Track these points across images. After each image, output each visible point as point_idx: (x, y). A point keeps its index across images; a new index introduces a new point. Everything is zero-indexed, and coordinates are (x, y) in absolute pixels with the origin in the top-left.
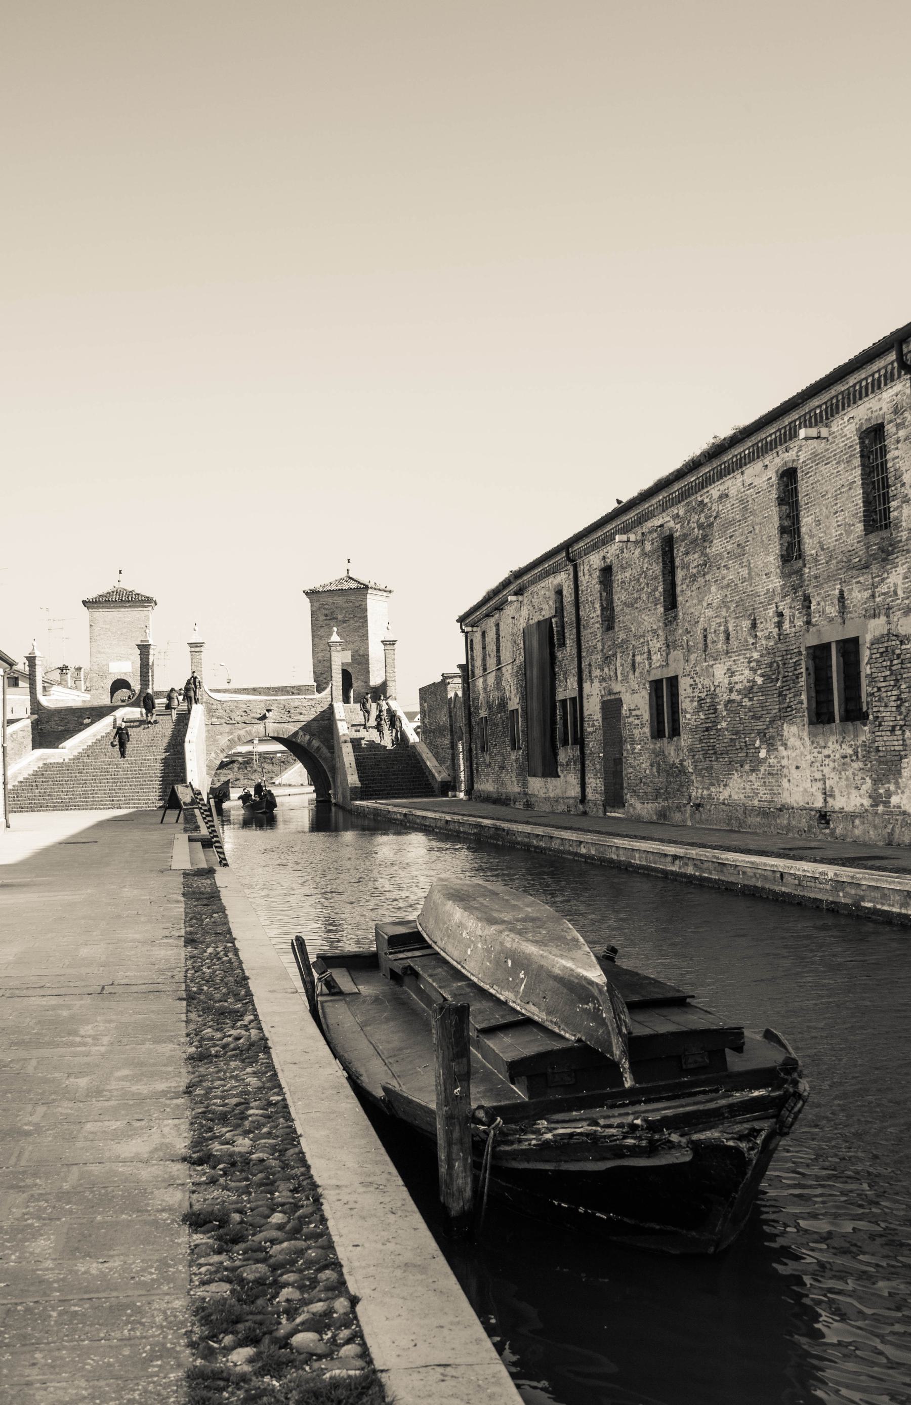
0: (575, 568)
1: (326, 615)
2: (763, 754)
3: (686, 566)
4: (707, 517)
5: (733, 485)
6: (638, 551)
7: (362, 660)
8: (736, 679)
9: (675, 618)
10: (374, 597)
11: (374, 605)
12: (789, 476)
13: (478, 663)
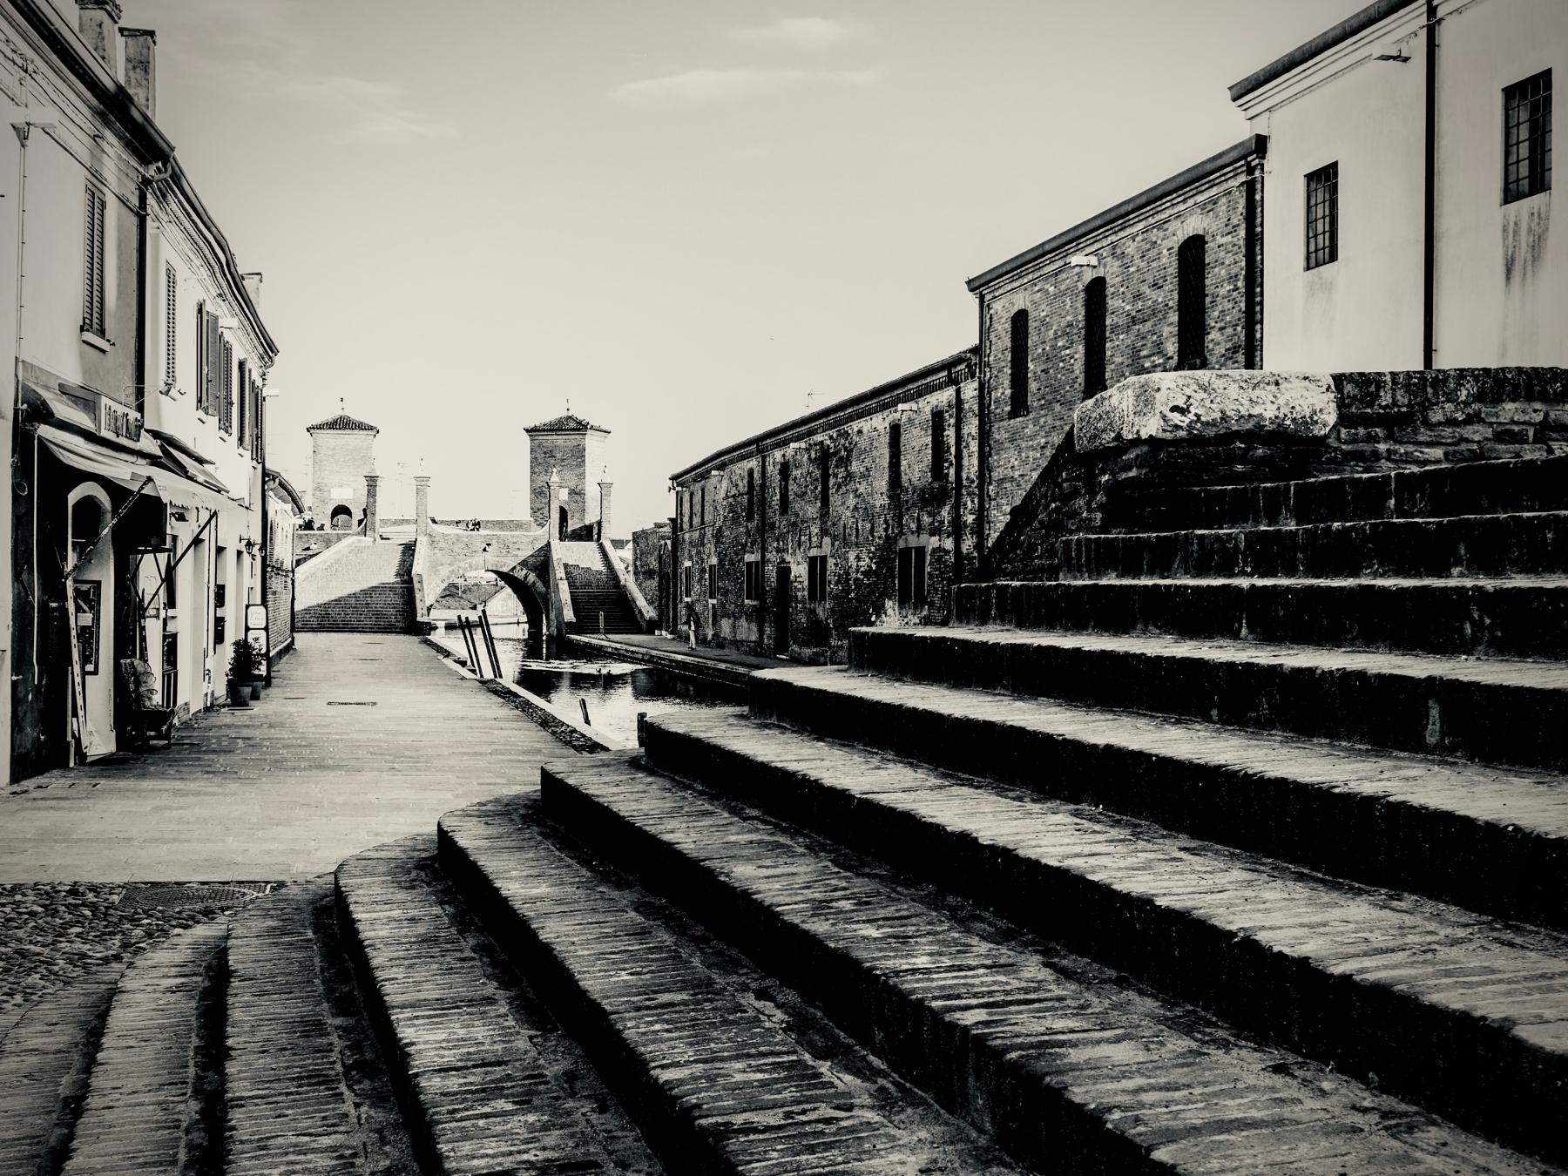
0: (764, 458)
1: (545, 453)
2: (873, 619)
3: (835, 476)
4: (850, 444)
5: (865, 424)
6: (806, 456)
7: (577, 493)
8: (862, 563)
9: (828, 512)
10: (593, 437)
11: (591, 441)
12: (895, 431)
13: (686, 519)
